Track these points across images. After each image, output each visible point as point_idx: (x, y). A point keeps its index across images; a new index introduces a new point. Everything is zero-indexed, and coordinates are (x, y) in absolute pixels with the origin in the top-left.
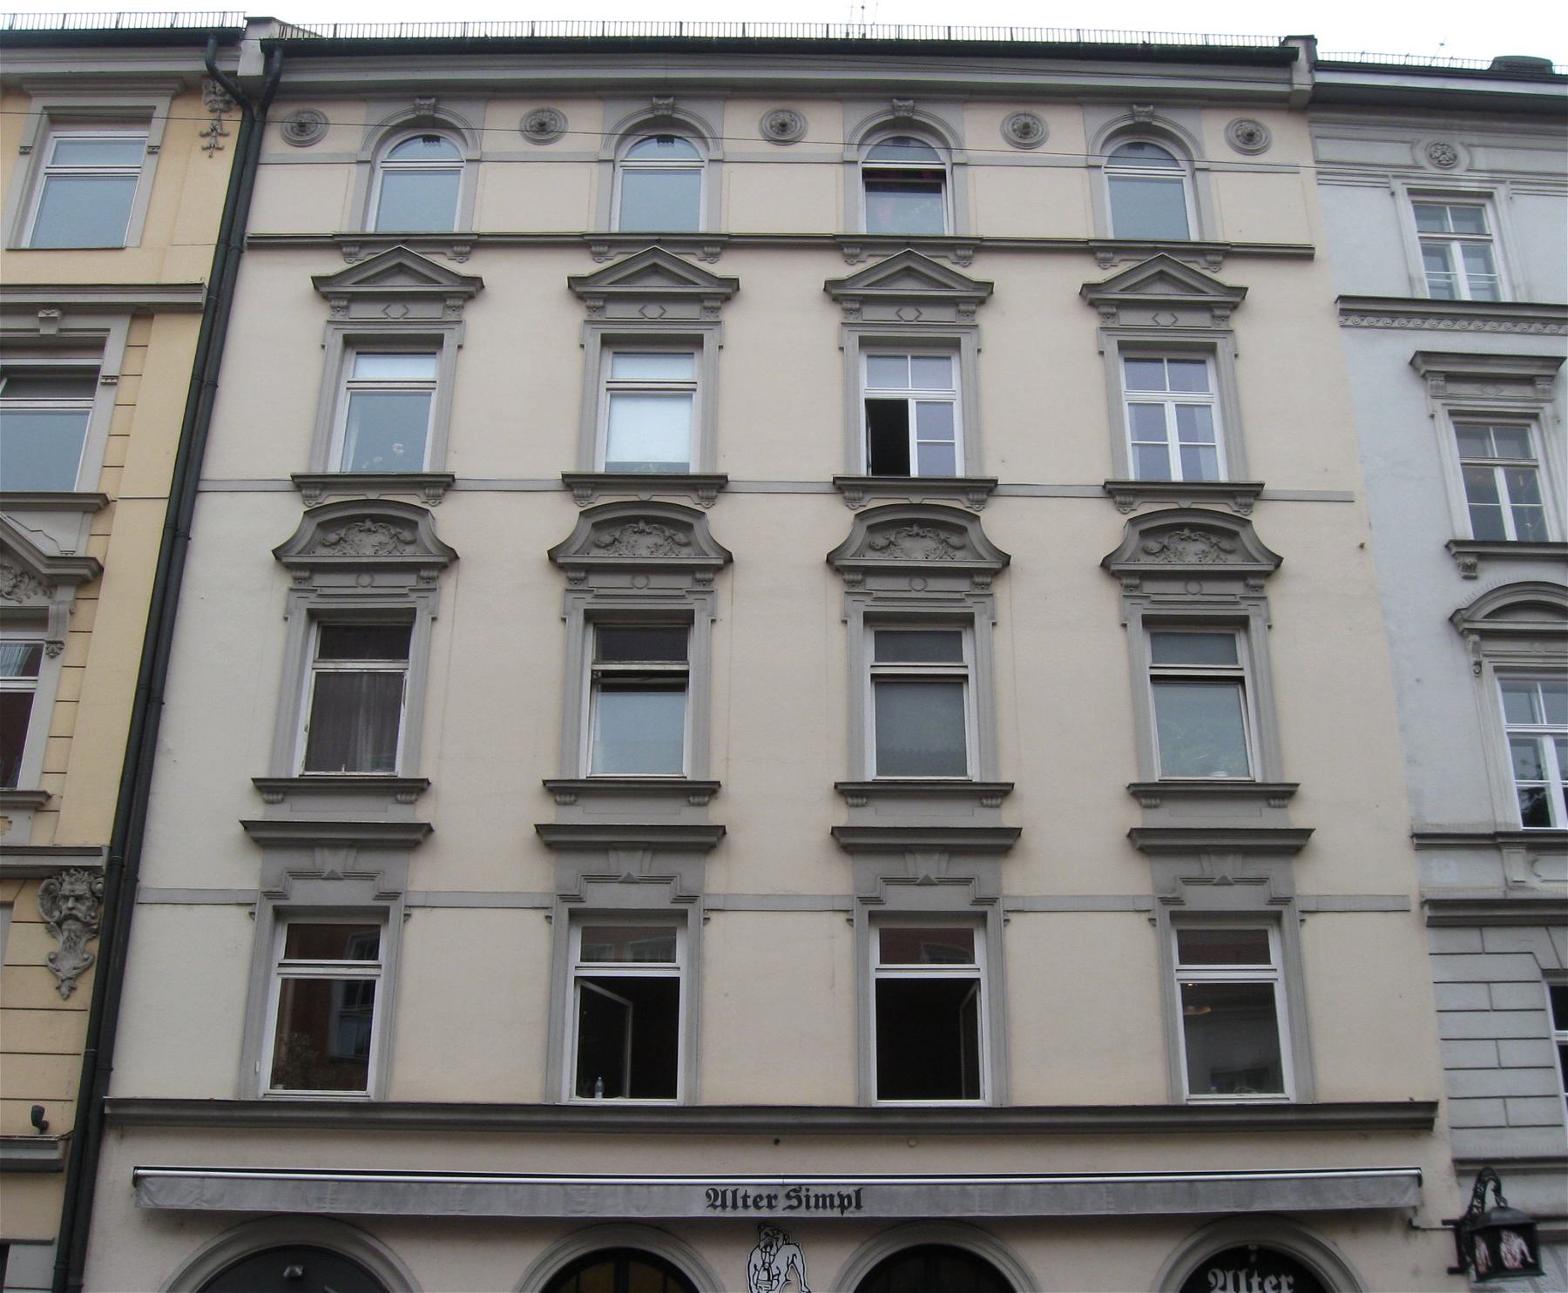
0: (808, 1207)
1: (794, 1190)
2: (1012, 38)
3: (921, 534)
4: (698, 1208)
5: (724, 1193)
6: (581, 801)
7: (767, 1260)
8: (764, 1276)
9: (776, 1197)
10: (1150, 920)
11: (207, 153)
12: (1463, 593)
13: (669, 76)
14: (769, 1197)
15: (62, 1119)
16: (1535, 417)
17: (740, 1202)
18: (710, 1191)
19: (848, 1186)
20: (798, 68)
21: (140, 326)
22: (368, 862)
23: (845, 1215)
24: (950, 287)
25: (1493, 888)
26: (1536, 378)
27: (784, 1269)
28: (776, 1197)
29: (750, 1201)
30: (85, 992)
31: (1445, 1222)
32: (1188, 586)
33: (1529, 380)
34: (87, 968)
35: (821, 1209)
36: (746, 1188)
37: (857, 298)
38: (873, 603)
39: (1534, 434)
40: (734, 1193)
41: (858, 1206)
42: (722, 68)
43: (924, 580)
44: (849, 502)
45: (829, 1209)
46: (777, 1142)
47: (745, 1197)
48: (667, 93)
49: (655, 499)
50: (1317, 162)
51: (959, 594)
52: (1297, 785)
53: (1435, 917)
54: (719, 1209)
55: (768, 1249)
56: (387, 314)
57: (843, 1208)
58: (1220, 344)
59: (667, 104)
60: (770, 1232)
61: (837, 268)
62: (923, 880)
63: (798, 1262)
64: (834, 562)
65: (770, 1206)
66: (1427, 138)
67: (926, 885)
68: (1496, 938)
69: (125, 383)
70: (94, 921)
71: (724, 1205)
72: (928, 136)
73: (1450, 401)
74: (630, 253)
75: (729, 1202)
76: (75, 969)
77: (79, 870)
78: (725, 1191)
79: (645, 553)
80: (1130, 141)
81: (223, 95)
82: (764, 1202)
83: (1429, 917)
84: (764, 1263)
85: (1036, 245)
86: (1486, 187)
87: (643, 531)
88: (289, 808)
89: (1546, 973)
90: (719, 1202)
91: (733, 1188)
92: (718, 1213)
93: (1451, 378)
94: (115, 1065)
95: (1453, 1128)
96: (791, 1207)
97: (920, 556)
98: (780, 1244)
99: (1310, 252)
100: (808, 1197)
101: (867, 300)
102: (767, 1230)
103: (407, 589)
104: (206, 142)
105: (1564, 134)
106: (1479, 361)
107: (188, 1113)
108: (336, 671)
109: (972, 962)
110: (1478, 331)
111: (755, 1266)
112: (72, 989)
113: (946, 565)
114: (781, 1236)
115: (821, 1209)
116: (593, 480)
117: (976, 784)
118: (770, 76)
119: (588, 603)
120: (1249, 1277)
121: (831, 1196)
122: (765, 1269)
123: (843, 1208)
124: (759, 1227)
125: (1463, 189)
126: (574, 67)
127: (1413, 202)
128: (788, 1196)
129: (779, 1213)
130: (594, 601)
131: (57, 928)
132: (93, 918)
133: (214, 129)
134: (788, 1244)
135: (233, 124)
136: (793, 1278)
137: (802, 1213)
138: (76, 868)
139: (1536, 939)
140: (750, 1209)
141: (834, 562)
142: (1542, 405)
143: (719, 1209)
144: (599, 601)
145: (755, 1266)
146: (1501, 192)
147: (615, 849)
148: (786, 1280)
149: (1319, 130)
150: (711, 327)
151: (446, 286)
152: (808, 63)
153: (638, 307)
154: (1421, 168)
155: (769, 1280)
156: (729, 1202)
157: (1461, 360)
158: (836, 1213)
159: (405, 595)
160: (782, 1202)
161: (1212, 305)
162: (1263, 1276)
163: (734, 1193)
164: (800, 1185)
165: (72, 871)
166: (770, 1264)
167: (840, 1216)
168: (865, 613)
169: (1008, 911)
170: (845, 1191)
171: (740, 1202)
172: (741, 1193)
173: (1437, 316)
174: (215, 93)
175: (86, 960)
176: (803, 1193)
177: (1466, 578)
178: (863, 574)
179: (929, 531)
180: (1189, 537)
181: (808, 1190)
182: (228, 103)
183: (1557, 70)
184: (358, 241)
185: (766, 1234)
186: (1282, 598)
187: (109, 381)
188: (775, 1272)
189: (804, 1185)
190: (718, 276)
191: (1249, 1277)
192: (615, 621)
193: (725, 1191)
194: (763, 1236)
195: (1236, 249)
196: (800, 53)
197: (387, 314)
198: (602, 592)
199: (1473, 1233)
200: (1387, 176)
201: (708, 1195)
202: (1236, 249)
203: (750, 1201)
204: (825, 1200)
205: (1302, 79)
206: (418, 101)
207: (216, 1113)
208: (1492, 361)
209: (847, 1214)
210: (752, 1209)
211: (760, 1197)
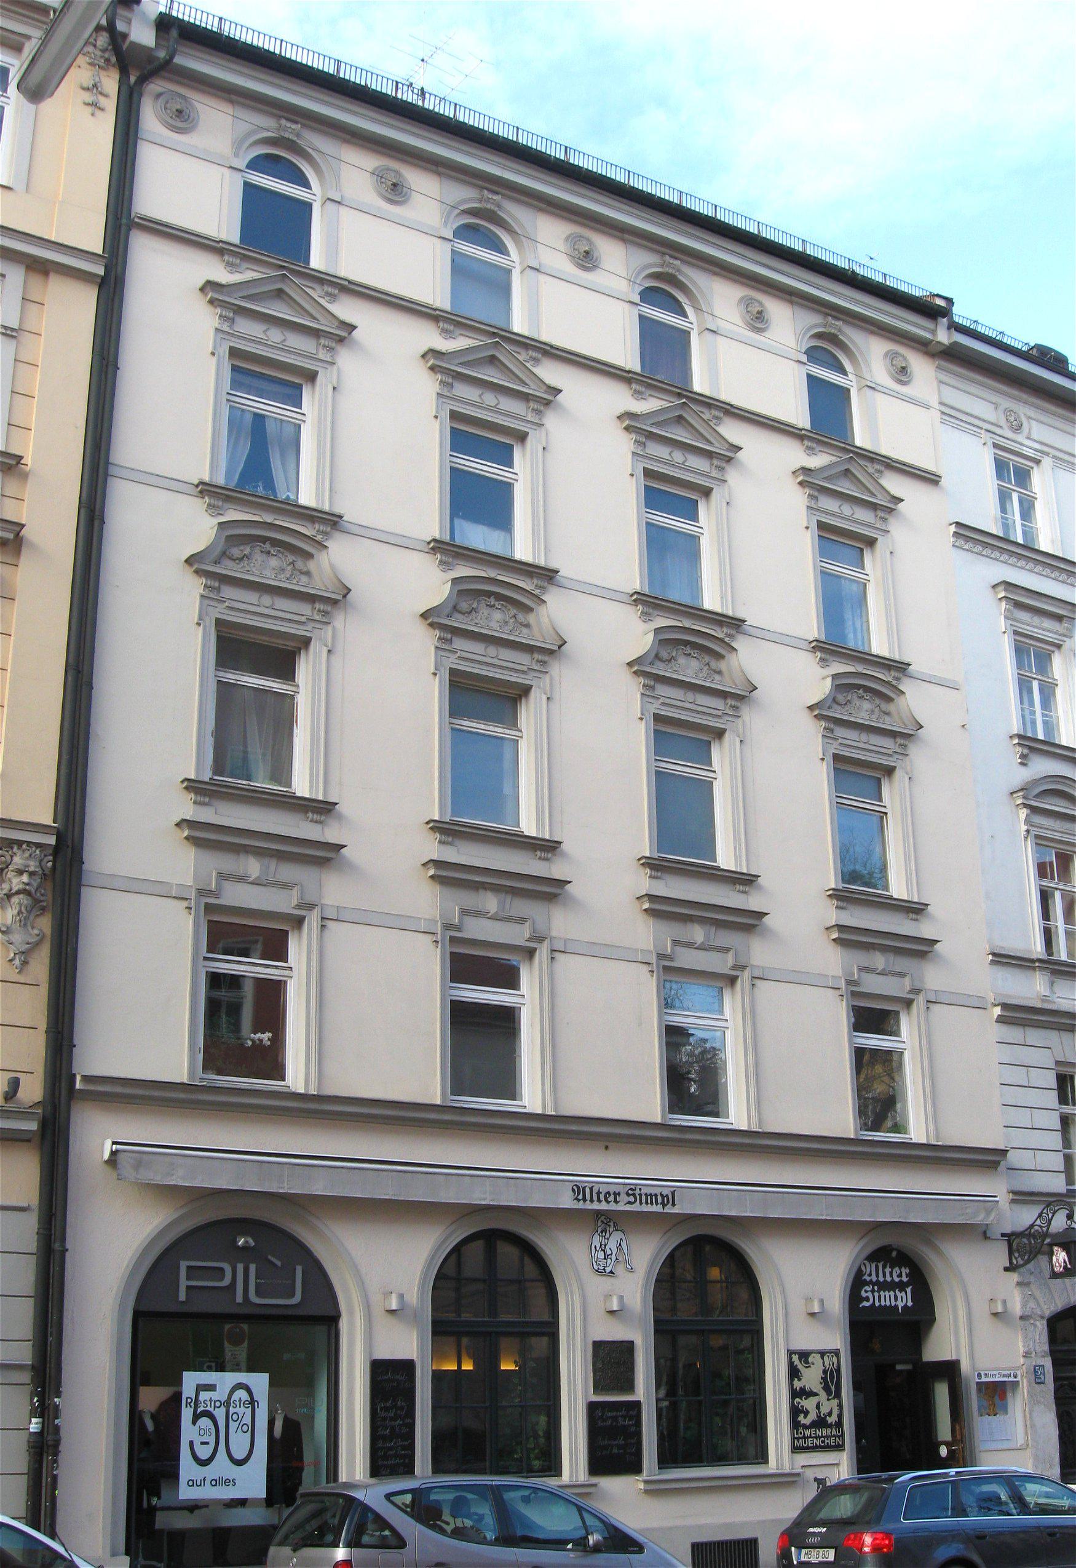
0: (641, 1203)
1: (631, 1189)
2: (716, 216)
3: (693, 654)
4: (567, 1201)
5: (584, 1188)
6: (457, 842)
7: (603, 1243)
8: (601, 1255)
9: (619, 1194)
10: (650, 971)
11: (90, 109)
12: (1023, 775)
13: (504, 176)
14: (615, 1193)
15: (32, 1091)
16: (1059, 647)
17: (595, 1197)
18: (574, 1187)
19: (665, 1189)
20: (606, 205)
21: (36, 281)
22: (288, 872)
23: (665, 1211)
24: (710, 443)
25: (1032, 999)
26: (1065, 619)
27: (615, 1251)
28: (619, 1194)
29: (602, 1197)
30: (41, 967)
31: (1003, 1235)
32: (862, 735)
33: (1059, 618)
34: (38, 944)
35: (649, 1205)
36: (599, 1185)
37: (644, 432)
38: (457, 661)
39: (1057, 660)
40: (591, 1189)
41: (674, 1204)
42: (545, 182)
43: (272, 598)
44: (646, 616)
45: (596, 1202)
46: (607, 1147)
47: (599, 1193)
48: (296, 118)
49: (500, 578)
50: (941, 403)
51: (717, 711)
52: (928, 905)
53: (1003, 1016)
54: (582, 1202)
55: (604, 1234)
56: (267, 337)
57: (664, 1205)
58: (880, 539)
59: (294, 129)
60: (604, 1222)
61: (432, 338)
62: (700, 945)
63: (624, 1244)
64: (638, 667)
65: (616, 1202)
66: (1006, 403)
67: (701, 949)
68: (1034, 1036)
69: (26, 338)
70: (42, 898)
71: (584, 1200)
72: (680, 293)
73: (1016, 624)
74: (265, 273)
75: (588, 1197)
76: (28, 944)
77: (31, 845)
78: (585, 1187)
79: (496, 626)
80: (652, 284)
81: (104, 51)
82: (611, 1198)
83: (999, 1015)
84: (601, 1245)
85: (749, 415)
86: (1037, 455)
87: (494, 606)
88: (214, 811)
89: (1058, 1063)
90: (581, 1197)
91: (590, 1185)
92: (580, 1205)
93: (1018, 605)
94: (77, 1040)
95: (1008, 1169)
96: (629, 1203)
97: (690, 672)
98: (611, 1229)
99: (938, 479)
100: (640, 1195)
101: (651, 436)
102: (603, 1218)
103: (305, 617)
104: (88, 97)
105: (1073, 422)
106: (1036, 597)
107: (157, 1093)
108: (235, 682)
109: (518, 989)
110: (1031, 571)
111: (595, 1247)
112: (25, 963)
113: (708, 685)
114: (612, 1224)
115: (649, 1205)
116: (455, 549)
117: (526, 837)
118: (521, 182)
119: (452, 662)
120: (884, 1267)
121: (656, 1195)
122: (602, 1250)
123: (664, 1205)
124: (597, 1216)
125: (1024, 452)
126: (280, 87)
127: (995, 454)
128: (628, 1194)
129: (621, 1207)
130: (838, 747)
131: (6, 900)
132: (42, 895)
133: (95, 86)
134: (617, 1230)
135: (111, 83)
136: (621, 1259)
137: (636, 1207)
138: (29, 843)
139: (1053, 1038)
140: (611, 1203)
141: (638, 667)
142: (1065, 639)
143: (582, 1202)
144: (842, 748)
145: (595, 1247)
146: (1047, 462)
147: (247, 852)
148: (617, 1259)
149: (943, 377)
150: (718, 483)
151: (324, 325)
152: (479, 153)
153: (264, 327)
154: (1001, 427)
155: (605, 1259)
156: (588, 1197)
157: (1027, 594)
158: (658, 1208)
159: (303, 623)
160: (623, 1198)
161: (878, 506)
162: (892, 1267)
163: (591, 1189)
164: (636, 1185)
165: (24, 846)
166: (605, 1246)
167: (662, 1210)
168: (833, 754)
169: (754, 977)
170: (665, 1192)
171: (595, 1197)
172: (595, 1190)
173: (992, 547)
174: (95, 46)
175: (38, 935)
176: (637, 1192)
177: (1021, 763)
178: (654, 680)
179: (279, 551)
180: (690, 654)
181: (640, 1189)
182: (107, 61)
183: (1072, 369)
184: (240, 253)
185: (602, 1221)
186: (919, 758)
187: (9, 332)
188: (609, 1252)
189: (640, 1185)
190: (547, 383)
191: (884, 1267)
192: (462, 681)
193: (585, 1187)
194: (600, 1224)
195: (896, 465)
196: (462, 137)
197: (267, 337)
198: (846, 742)
199: (1051, 1245)
200: (981, 428)
201: (573, 1190)
202: (896, 465)
203: (602, 1197)
204: (651, 1198)
205: (943, 336)
206: (284, 122)
207: (182, 1096)
208: (1044, 599)
209: (666, 1210)
210: (604, 1203)
211: (608, 1193)
